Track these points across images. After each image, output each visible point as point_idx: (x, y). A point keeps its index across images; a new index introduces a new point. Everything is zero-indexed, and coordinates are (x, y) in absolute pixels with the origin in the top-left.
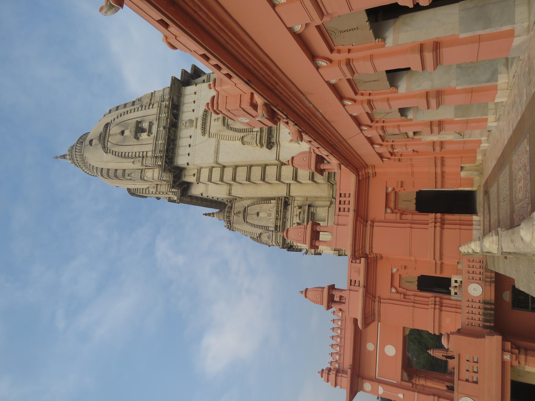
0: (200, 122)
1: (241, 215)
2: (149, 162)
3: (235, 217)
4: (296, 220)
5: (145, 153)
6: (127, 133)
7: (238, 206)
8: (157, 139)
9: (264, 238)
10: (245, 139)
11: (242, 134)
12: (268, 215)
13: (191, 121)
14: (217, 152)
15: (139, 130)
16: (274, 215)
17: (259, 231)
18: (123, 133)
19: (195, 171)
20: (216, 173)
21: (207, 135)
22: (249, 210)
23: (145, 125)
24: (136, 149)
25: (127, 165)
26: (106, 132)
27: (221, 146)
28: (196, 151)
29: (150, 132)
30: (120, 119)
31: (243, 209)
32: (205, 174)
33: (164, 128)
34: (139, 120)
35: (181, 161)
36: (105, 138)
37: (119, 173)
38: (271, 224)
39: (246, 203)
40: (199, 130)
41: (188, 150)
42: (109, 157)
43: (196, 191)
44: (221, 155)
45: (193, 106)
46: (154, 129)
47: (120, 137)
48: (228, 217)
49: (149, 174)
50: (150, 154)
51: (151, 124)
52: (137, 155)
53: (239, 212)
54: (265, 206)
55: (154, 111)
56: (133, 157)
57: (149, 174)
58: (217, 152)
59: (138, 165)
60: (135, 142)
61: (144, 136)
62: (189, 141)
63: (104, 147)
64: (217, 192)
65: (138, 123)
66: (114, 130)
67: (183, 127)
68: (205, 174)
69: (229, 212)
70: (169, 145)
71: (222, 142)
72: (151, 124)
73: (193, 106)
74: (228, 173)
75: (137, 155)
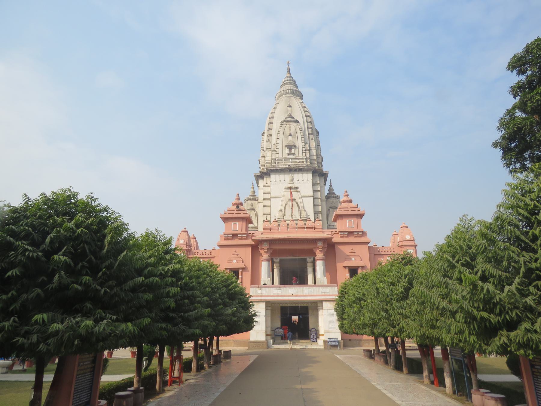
0: (292, 185)
1: (251, 207)
2: (274, 156)
3: (250, 203)
5: (277, 152)
6: (290, 137)
8: (285, 159)
10: (281, 212)
11: (283, 210)
13: (293, 180)
14: (276, 197)
15: (290, 147)
18: (290, 135)
19: (269, 184)
20: (267, 196)
21: (285, 190)
24: (280, 147)
25: (274, 139)
26: (292, 121)
27: (279, 199)
28: (278, 184)
29: (289, 154)
30: (299, 132)
31: (254, 207)
32: (267, 189)
33: (289, 166)
34: (297, 145)
35: (273, 177)
36: (289, 121)
42: (279, 125)
45: (301, 179)
47: (287, 133)
48: (250, 199)
51: (294, 154)
52: (277, 147)
53: (252, 206)
55: (301, 155)
57: (268, 154)
58: (276, 197)
59: (273, 147)
61: (287, 151)
62: (282, 181)
63: (283, 122)
65: (295, 146)
67: (290, 175)
68: (267, 189)
69: (253, 199)
70: (280, 169)
72: (294, 154)
73: (301, 179)
74: (267, 203)
75: (277, 147)
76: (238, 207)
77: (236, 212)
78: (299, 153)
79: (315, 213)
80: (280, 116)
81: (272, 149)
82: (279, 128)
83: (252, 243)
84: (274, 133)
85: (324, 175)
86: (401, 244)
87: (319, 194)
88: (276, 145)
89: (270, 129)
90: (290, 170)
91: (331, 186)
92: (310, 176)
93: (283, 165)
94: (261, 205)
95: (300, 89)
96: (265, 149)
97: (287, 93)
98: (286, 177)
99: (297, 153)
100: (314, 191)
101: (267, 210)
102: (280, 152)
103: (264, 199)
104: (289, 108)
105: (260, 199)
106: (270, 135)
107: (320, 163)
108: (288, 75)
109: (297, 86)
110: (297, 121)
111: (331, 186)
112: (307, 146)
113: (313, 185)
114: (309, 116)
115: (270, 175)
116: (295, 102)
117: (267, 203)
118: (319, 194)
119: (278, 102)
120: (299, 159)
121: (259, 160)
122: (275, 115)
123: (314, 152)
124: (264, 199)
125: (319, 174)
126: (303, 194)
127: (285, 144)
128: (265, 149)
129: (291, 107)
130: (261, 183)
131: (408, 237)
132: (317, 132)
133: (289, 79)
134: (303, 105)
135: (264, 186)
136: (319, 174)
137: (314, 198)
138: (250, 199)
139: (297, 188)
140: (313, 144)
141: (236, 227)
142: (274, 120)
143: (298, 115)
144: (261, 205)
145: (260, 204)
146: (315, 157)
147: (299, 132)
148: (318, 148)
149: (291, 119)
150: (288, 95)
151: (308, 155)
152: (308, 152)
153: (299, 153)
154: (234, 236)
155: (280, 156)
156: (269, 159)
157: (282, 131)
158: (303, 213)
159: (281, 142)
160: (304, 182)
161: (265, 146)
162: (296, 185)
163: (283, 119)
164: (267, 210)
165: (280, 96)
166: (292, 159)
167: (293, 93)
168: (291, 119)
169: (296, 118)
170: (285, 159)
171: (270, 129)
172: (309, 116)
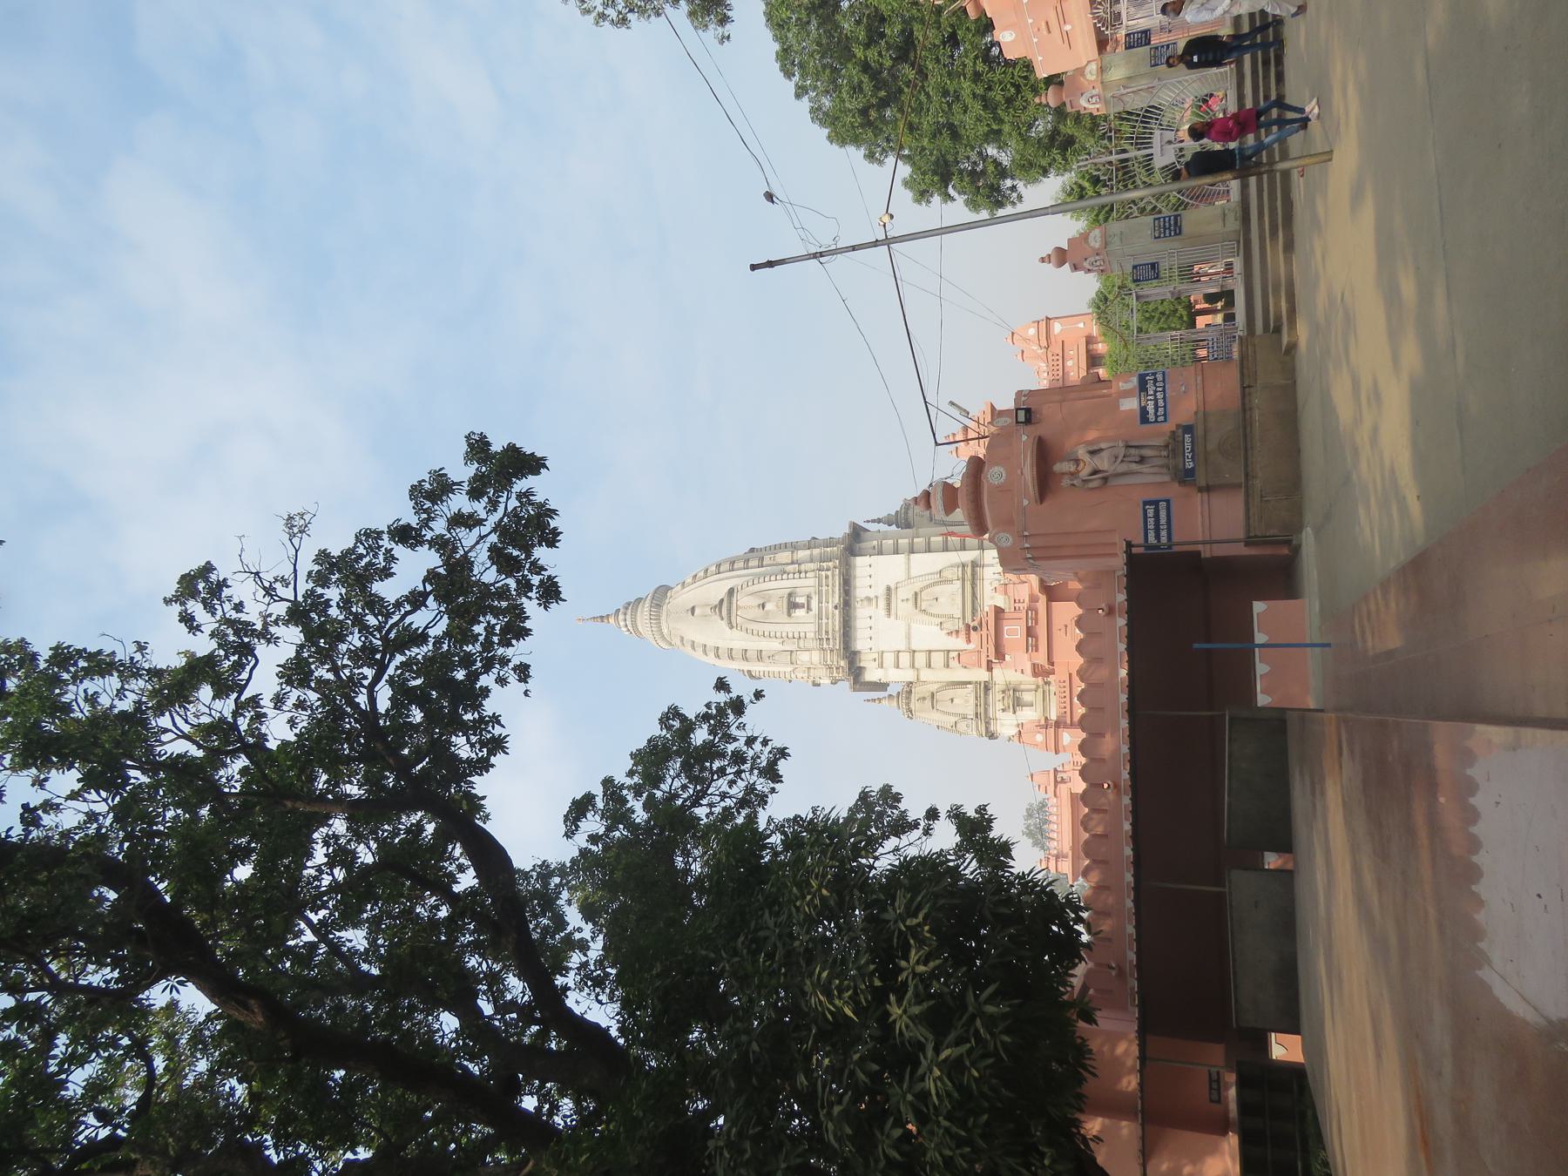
0: (882, 603)
1: (928, 702)
4: (1000, 706)
6: (769, 607)
7: (918, 691)
8: (820, 618)
9: (962, 726)
12: (965, 701)
13: (869, 599)
14: (909, 637)
15: (793, 606)
16: (972, 701)
17: (953, 719)
20: (905, 659)
22: (938, 696)
23: (801, 600)
24: (789, 629)
26: (730, 603)
28: (878, 635)
29: (809, 609)
30: (756, 588)
31: (928, 695)
32: (889, 659)
35: (861, 643)
37: (752, 654)
38: (971, 712)
39: (934, 688)
40: (882, 610)
41: (868, 633)
43: (872, 675)
44: (913, 641)
45: (868, 581)
46: (814, 604)
48: (908, 704)
49: (804, 657)
50: (811, 635)
54: (960, 691)
56: (784, 639)
58: (909, 637)
60: (787, 619)
61: (800, 613)
64: (896, 676)
65: (790, 595)
66: (742, 600)
68: (889, 659)
69: (908, 698)
71: (913, 625)
72: (809, 597)
73: (868, 581)
74: (921, 659)
76: (975, 629)
77: (984, 632)
78: (805, 585)
79: (946, 549)
80: (717, 633)
81: (794, 648)
82: (743, 634)
83: (1043, 599)
84: (753, 645)
85: (857, 533)
86: (1044, 343)
87: (903, 542)
88: (784, 639)
89: (745, 656)
90: (847, 605)
91: (879, 521)
92: (860, 562)
93: (835, 622)
94: (926, 675)
95: (647, 590)
96: (790, 669)
97: (658, 619)
98: (862, 614)
99: (807, 591)
100: (896, 552)
101: (938, 659)
102: (802, 628)
103: (913, 666)
104: (697, 611)
105: (909, 676)
106: (760, 656)
107: (829, 543)
108: (612, 620)
109: (639, 600)
110: (731, 592)
111: (879, 521)
112: (790, 568)
113: (880, 553)
114: (719, 566)
115: (856, 653)
116: (680, 599)
117: (921, 659)
118: (903, 542)
119: (677, 641)
120: (820, 585)
121: (815, 684)
122: (711, 643)
123: (802, 554)
124: (913, 666)
125: (855, 541)
126: (902, 576)
127: (785, 618)
128: (790, 669)
129: (693, 609)
130: (872, 675)
131: (1032, 331)
132: (752, 550)
133: (621, 617)
134: (689, 580)
135: (881, 666)
136: (855, 541)
137: (912, 551)
138: (908, 704)
139: (889, 589)
140: (784, 557)
141: (1014, 632)
142: (724, 645)
143: (716, 589)
144: (926, 675)
145: (922, 678)
146: (816, 552)
147: (756, 588)
148: (794, 547)
149: (725, 607)
150: (663, 618)
151: (812, 566)
152: (803, 567)
153: (805, 585)
154: (1030, 632)
155: (810, 630)
156: (816, 657)
157: (751, 626)
158: (948, 574)
159: (778, 628)
160: (873, 572)
161: (782, 669)
162: (881, 591)
163: (724, 624)
164: (938, 659)
165: (663, 637)
166: (820, 602)
167: (659, 606)
168: (725, 607)
169: (723, 593)
170: (820, 618)
171: (745, 656)
172: (719, 566)
